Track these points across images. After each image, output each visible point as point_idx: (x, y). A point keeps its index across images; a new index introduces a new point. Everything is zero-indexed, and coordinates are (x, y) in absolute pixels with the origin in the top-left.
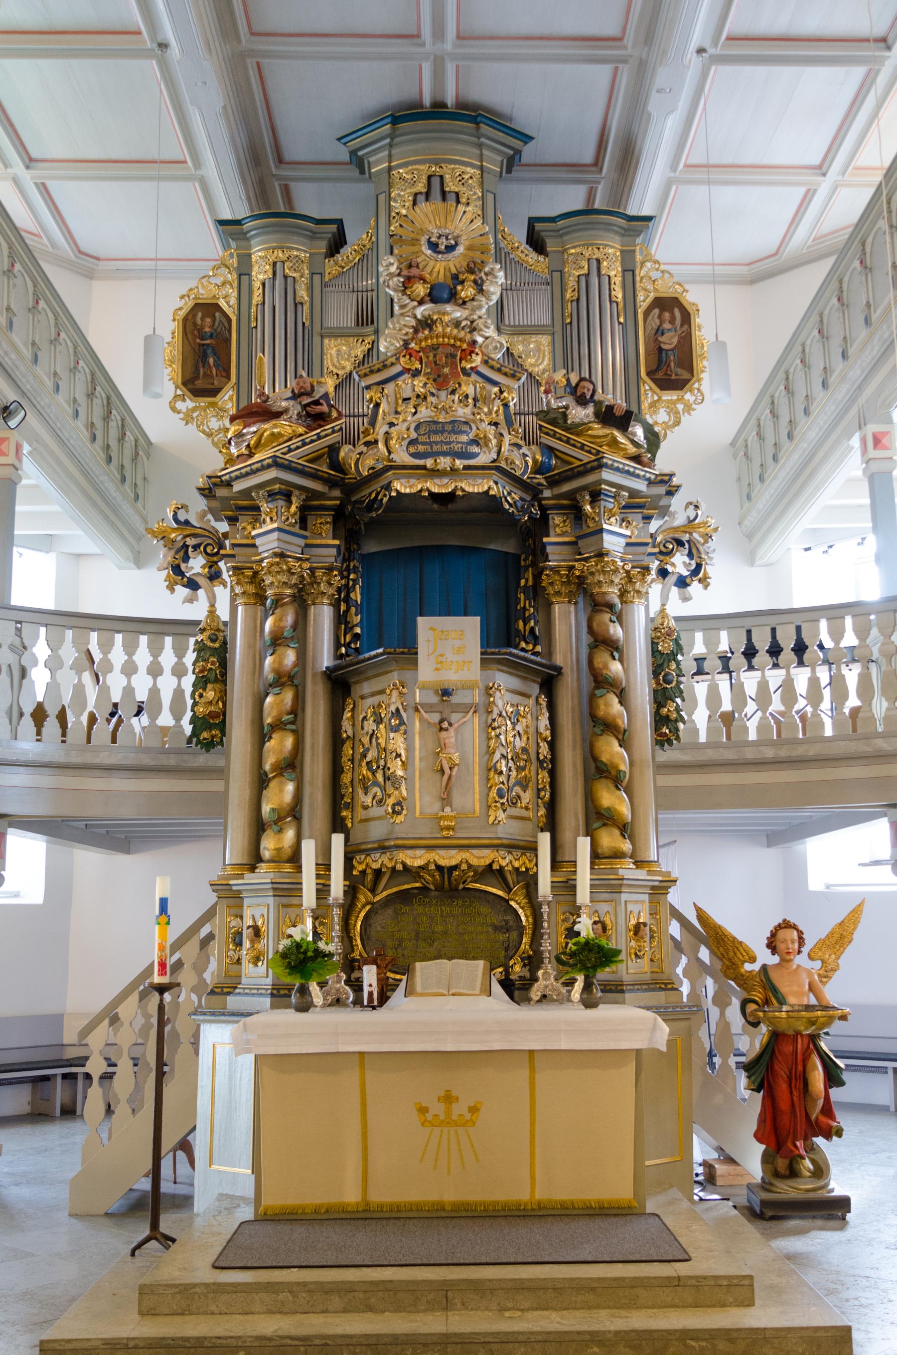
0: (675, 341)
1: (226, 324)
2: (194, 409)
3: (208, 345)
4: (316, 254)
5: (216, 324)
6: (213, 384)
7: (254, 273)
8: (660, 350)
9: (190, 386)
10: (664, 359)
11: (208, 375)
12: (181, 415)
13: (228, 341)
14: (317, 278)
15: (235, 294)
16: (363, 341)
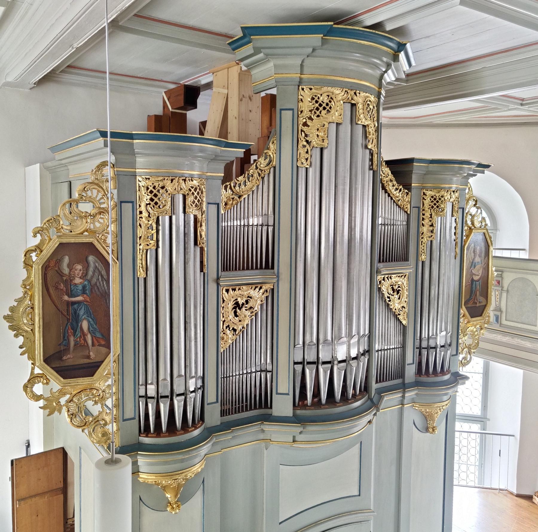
0: (481, 272)
1: (104, 273)
2: (62, 393)
3: (79, 303)
4: (213, 178)
5: (90, 273)
6: (88, 357)
7: (143, 205)
8: (473, 280)
9: (57, 364)
10: (474, 289)
11: (82, 346)
12: (41, 403)
13: (106, 295)
14: (214, 208)
15: (112, 228)
16: (261, 288)
